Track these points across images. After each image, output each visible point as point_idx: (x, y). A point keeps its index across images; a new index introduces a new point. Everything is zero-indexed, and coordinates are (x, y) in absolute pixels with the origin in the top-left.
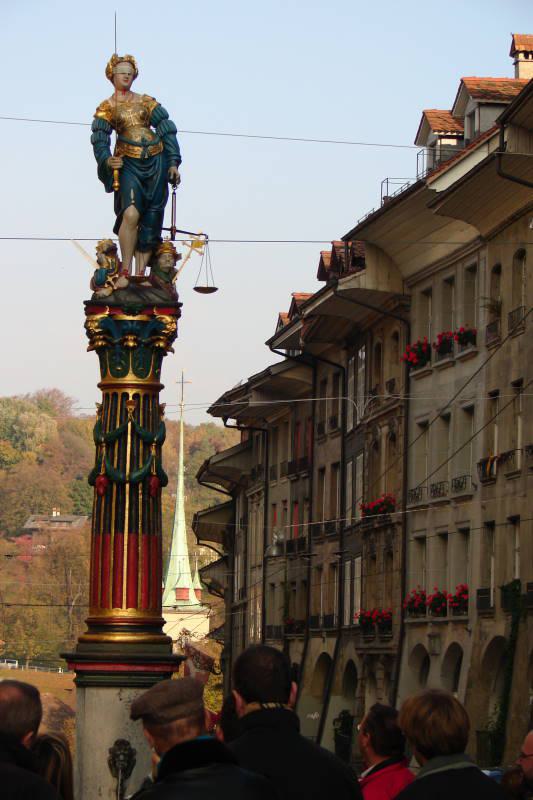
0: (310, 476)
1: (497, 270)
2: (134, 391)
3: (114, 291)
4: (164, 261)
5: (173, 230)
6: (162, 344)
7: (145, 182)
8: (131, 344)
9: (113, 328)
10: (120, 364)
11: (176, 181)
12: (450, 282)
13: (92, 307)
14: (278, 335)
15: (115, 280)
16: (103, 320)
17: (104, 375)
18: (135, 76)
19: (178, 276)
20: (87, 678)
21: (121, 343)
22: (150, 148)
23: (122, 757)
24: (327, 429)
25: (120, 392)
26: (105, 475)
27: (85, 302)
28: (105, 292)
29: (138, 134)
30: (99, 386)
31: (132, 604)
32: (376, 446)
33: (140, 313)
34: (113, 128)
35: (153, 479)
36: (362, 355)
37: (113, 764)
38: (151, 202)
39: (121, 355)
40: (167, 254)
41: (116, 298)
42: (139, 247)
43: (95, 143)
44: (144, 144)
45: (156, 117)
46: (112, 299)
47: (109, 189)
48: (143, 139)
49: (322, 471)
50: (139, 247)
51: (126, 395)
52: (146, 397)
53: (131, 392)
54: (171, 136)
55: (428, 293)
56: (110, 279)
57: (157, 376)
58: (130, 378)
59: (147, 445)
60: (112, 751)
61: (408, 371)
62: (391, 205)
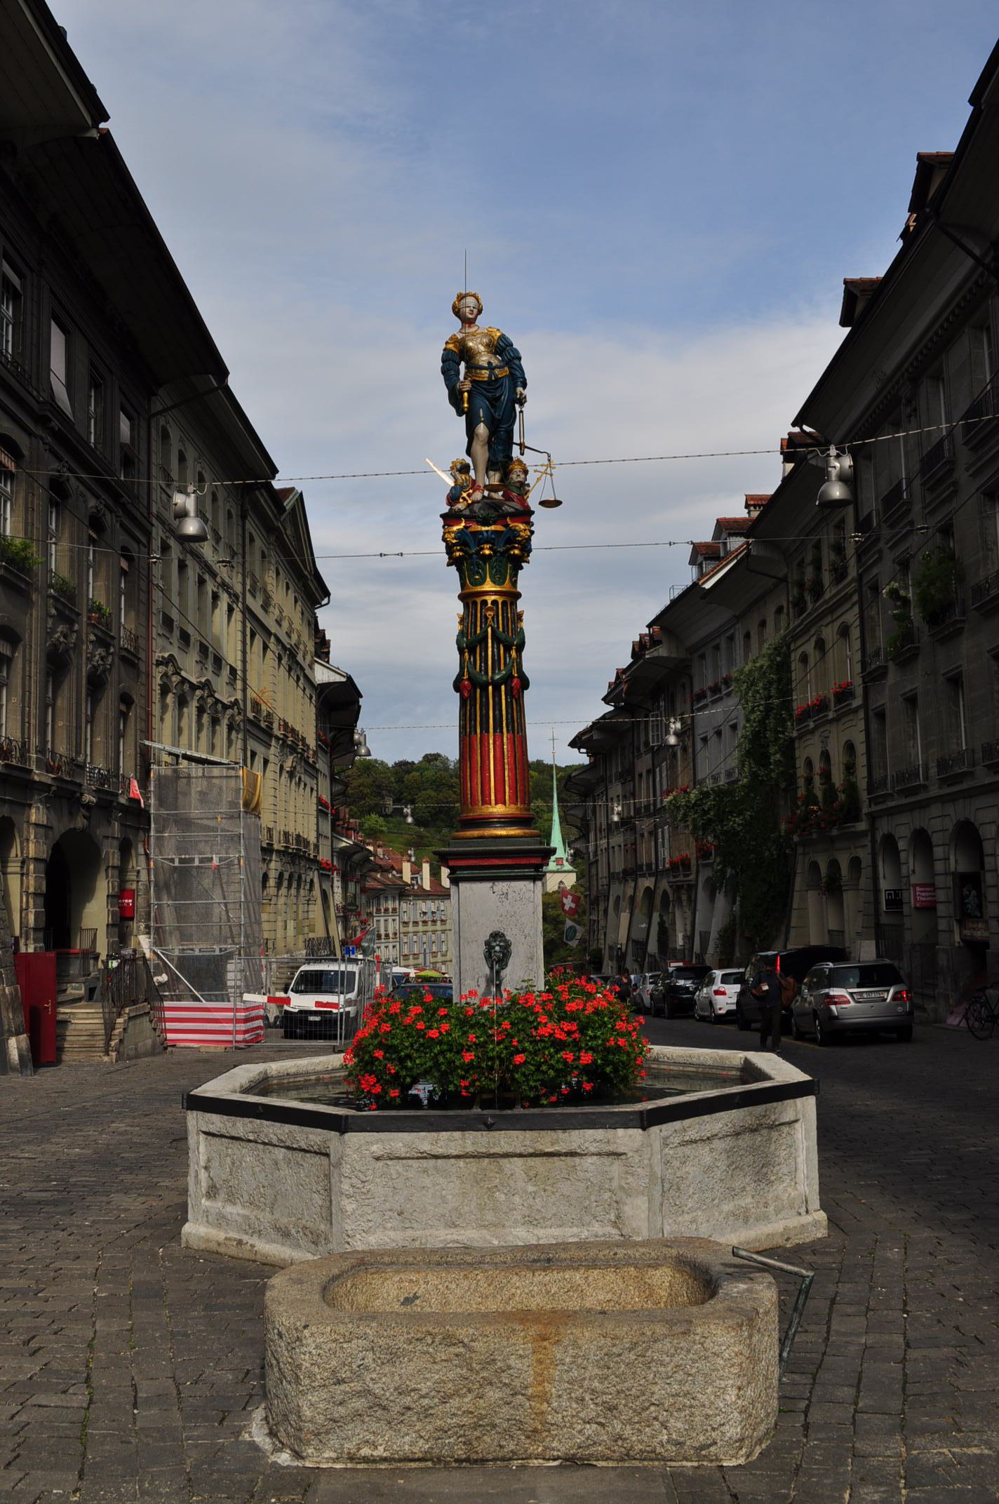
0: (633, 780)
1: (747, 636)
2: (493, 598)
3: (469, 505)
4: (516, 477)
5: (522, 446)
6: (517, 552)
7: (494, 402)
8: (487, 552)
9: (470, 540)
10: (478, 573)
11: (522, 401)
12: (717, 648)
13: (449, 518)
14: (609, 694)
15: (469, 495)
16: (459, 531)
17: (463, 585)
18: (480, 311)
19: (530, 495)
20: (459, 874)
21: (477, 553)
22: (497, 371)
23: (497, 948)
24: (642, 749)
25: (479, 600)
26: (470, 679)
27: (442, 516)
28: (461, 506)
29: (484, 359)
30: (461, 597)
31: (500, 800)
32: (674, 755)
33: (495, 523)
34: (462, 359)
35: (515, 681)
36: (662, 703)
37: (489, 955)
38: (499, 421)
39: (478, 565)
40: (517, 468)
41: (471, 511)
42: (491, 466)
43: (444, 372)
44: (490, 367)
45: (502, 348)
46: (467, 512)
47: (460, 413)
48: (489, 363)
49: (640, 775)
50: (491, 466)
51: (485, 602)
52: (504, 603)
53: (490, 599)
54: (516, 362)
55: (703, 657)
56: (464, 495)
57: (514, 584)
58: (488, 586)
59: (508, 649)
60: (487, 943)
61: (692, 705)
62: (674, 603)
